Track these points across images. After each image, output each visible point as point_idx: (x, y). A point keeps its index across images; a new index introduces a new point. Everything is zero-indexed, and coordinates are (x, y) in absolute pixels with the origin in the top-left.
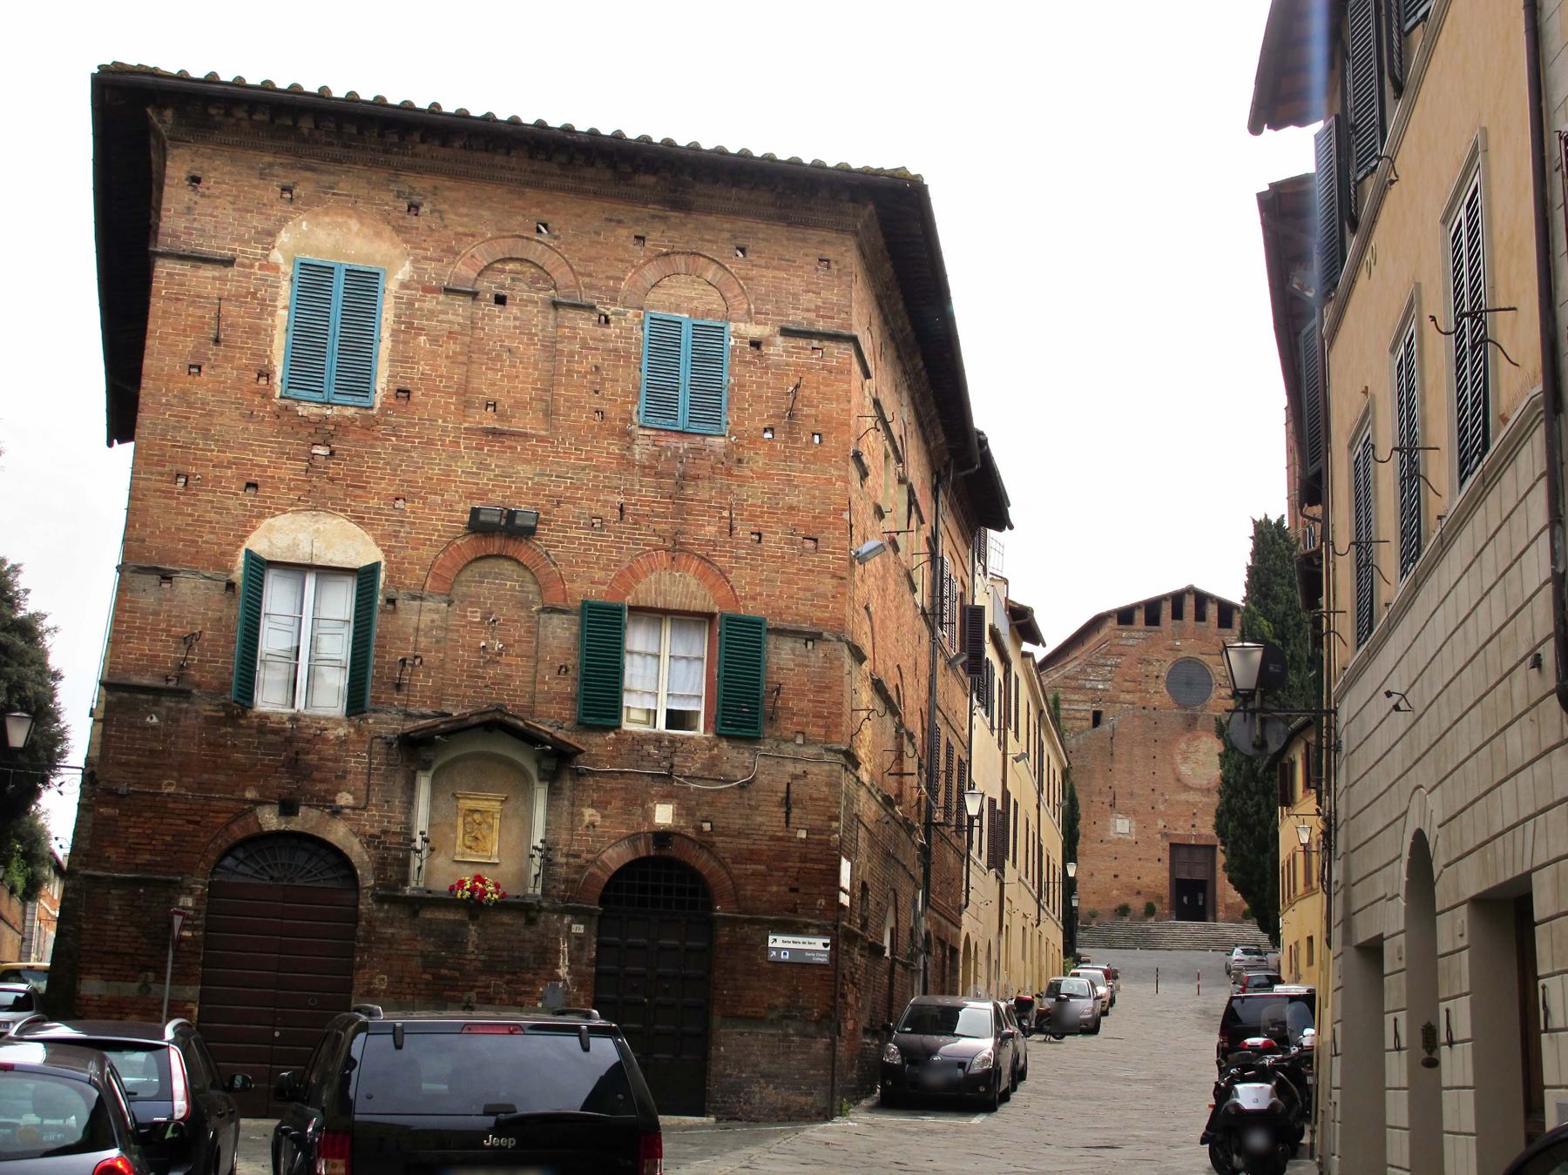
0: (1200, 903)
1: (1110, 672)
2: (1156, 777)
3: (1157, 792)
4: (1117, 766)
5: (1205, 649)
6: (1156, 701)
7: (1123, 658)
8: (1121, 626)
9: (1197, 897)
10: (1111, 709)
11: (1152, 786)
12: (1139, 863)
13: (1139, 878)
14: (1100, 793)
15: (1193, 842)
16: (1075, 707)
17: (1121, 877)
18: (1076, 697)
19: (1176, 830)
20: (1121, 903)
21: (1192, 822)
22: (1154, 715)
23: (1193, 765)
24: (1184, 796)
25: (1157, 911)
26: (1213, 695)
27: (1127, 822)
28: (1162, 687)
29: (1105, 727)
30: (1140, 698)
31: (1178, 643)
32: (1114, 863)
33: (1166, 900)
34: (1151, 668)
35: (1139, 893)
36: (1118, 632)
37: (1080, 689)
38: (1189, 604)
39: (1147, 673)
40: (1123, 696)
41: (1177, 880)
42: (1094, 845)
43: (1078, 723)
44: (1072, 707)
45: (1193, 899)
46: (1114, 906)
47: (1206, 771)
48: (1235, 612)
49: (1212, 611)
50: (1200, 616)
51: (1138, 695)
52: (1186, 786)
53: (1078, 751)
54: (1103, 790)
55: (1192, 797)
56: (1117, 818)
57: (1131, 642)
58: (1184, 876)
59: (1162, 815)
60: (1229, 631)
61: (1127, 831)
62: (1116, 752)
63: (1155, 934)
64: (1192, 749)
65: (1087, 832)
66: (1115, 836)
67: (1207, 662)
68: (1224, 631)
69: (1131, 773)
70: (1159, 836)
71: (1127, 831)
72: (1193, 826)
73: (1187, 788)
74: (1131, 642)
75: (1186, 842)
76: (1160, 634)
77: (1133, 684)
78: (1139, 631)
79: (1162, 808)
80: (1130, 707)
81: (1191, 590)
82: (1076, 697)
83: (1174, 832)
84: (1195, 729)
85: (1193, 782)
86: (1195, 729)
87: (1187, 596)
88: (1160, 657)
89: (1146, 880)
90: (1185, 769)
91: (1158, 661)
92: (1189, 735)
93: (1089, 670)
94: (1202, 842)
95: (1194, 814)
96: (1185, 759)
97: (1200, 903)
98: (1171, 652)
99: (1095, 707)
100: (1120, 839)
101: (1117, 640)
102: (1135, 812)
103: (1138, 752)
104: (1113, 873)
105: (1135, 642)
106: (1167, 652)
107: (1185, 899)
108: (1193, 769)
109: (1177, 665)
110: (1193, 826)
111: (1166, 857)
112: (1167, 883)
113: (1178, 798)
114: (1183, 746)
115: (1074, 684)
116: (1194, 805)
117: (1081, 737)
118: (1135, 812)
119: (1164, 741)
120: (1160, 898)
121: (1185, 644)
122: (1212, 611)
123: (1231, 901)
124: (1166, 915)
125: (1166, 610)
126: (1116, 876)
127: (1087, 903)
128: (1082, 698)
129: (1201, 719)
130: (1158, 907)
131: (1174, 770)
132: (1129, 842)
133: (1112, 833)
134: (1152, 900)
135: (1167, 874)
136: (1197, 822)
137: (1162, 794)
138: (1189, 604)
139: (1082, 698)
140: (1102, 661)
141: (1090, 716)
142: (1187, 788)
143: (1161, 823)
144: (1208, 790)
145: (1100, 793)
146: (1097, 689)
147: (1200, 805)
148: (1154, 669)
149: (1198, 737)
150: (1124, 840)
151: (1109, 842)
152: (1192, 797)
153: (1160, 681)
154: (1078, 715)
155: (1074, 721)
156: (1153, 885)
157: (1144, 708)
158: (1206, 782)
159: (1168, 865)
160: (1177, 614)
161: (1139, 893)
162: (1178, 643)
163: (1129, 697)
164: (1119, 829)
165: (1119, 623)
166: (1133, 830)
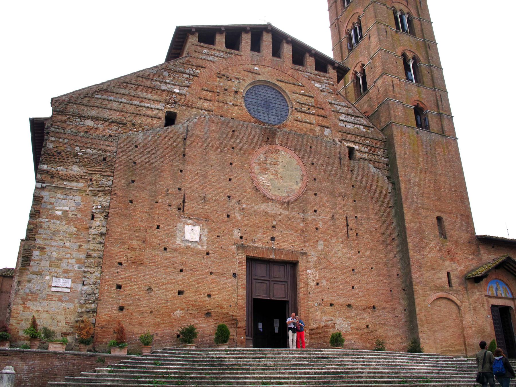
0: (277, 330)
1: (188, 79)
2: (232, 184)
3: (232, 200)
4: (189, 168)
5: (280, 78)
6: (235, 112)
7: (202, 70)
8: (202, 44)
9: (272, 324)
10: (186, 113)
11: (228, 193)
12: (213, 277)
13: (209, 296)
14: (167, 193)
15: (273, 257)
16: (147, 105)
17: (186, 294)
18: (149, 96)
19: (254, 242)
20: (185, 325)
21: (271, 235)
22: (232, 124)
23: (272, 177)
24: (263, 207)
25: (231, 337)
26: (290, 118)
27: (197, 229)
28: (240, 101)
29: (179, 128)
30: (218, 107)
31: (256, 68)
32: (180, 276)
33: (242, 324)
34: (229, 83)
35: (208, 314)
36: (198, 47)
37: (154, 89)
38: (267, 40)
39: (226, 88)
40: (200, 103)
41: (253, 298)
42: (155, 253)
43: (149, 120)
44: (144, 104)
45: (269, 326)
46: (176, 330)
47: (285, 184)
48: (307, 55)
49: (287, 50)
50: (276, 52)
51: (216, 104)
52: (264, 196)
53: (145, 146)
54: (170, 190)
55: (272, 208)
56: (185, 223)
57: (211, 58)
58: (261, 295)
59: (238, 225)
60: (302, 68)
61: (197, 239)
62: (189, 152)
63: (232, 367)
64: (270, 161)
65: (148, 236)
66: (183, 245)
67: (283, 88)
68: (297, 67)
69: (205, 177)
70: (234, 248)
71: (197, 239)
72: (273, 239)
73: (266, 199)
74: (211, 58)
75: (265, 256)
76: (239, 57)
77: (211, 94)
78: (220, 51)
79: (238, 217)
80: (207, 113)
81: (268, 29)
82: (149, 96)
83: (252, 244)
84: (274, 143)
85: (272, 193)
86: (274, 143)
87: (265, 34)
88: (239, 76)
89: (218, 298)
90: (263, 179)
91: (238, 79)
92: (267, 148)
93: (166, 74)
94: (283, 258)
95: (274, 227)
96: (264, 170)
97: (277, 330)
98: (250, 74)
99: (169, 108)
100: (188, 247)
101: (196, 55)
102: (207, 218)
103: (213, 156)
104: (178, 288)
105: (216, 59)
106: (246, 73)
107: (260, 326)
108: (271, 180)
109: (255, 85)
110: (273, 239)
111: (242, 271)
112: (243, 303)
113: (256, 208)
114: (262, 157)
115: (148, 83)
116: (274, 217)
117: (150, 133)
118: (207, 218)
119: (242, 149)
120: (234, 321)
121: (263, 70)
122: (287, 50)
123: (316, 326)
124: (242, 342)
125: (246, 40)
126: (180, 293)
127: (141, 324)
128: (156, 97)
129: (279, 135)
130: (232, 332)
131: (252, 180)
132: (199, 252)
133: (178, 241)
134: (224, 322)
135: (243, 292)
136: (276, 234)
137: (239, 203)
138: (267, 40)
139: (156, 97)
140: (180, 69)
141: (163, 116)
142: (266, 199)
143: (237, 234)
144: (288, 203)
145: (167, 193)
146: (172, 92)
147: (280, 217)
148: (234, 85)
149: (277, 151)
150: (194, 248)
151: (175, 250)
152: (272, 208)
153: (238, 96)
154: (149, 113)
155: (144, 118)
156: (226, 305)
157: (222, 116)
158: (285, 195)
159: (244, 282)
160: (256, 46)
161: (208, 314)
162: (256, 68)
163: (206, 105)
164: (188, 236)
165: (200, 41)
166: (205, 239)
